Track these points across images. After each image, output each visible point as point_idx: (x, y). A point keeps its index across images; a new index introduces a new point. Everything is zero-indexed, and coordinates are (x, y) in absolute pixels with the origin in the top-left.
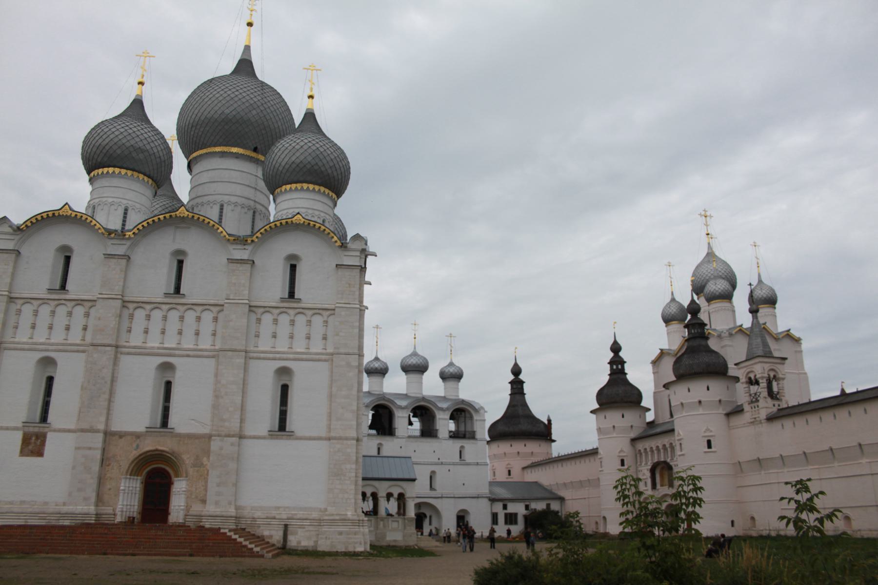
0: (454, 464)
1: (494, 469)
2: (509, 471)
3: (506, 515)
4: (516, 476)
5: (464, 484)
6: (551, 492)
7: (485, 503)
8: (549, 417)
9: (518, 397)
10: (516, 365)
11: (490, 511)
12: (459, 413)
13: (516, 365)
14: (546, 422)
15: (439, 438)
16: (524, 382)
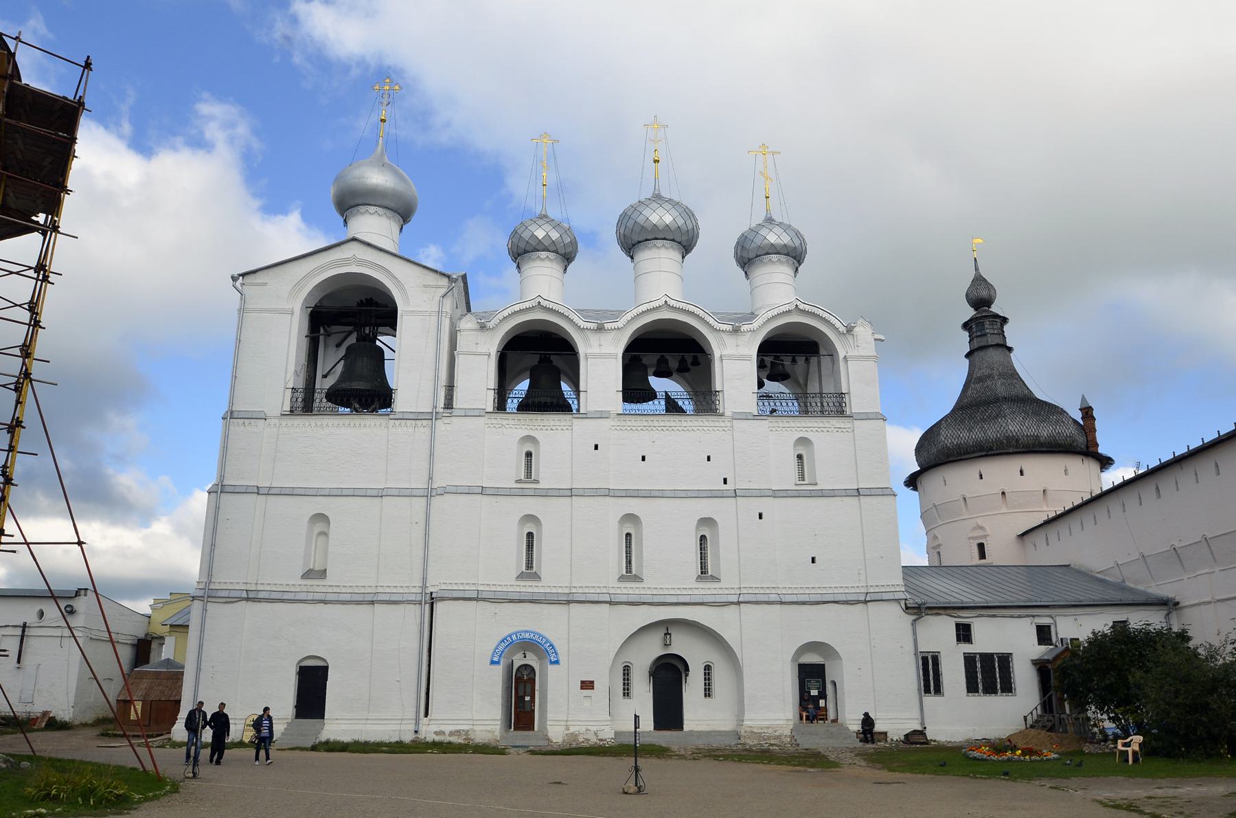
0: (775, 494)
1: (939, 545)
2: (981, 547)
3: (969, 660)
4: (1002, 551)
5: (813, 560)
6: (1121, 587)
7: (894, 619)
8: (1083, 398)
9: (994, 355)
10: (979, 280)
11: (910, 647)
12: (801, 360)
13: (979, 280)
14: (1078, 416)
15: (722, 415)
16: (1004, 320)
